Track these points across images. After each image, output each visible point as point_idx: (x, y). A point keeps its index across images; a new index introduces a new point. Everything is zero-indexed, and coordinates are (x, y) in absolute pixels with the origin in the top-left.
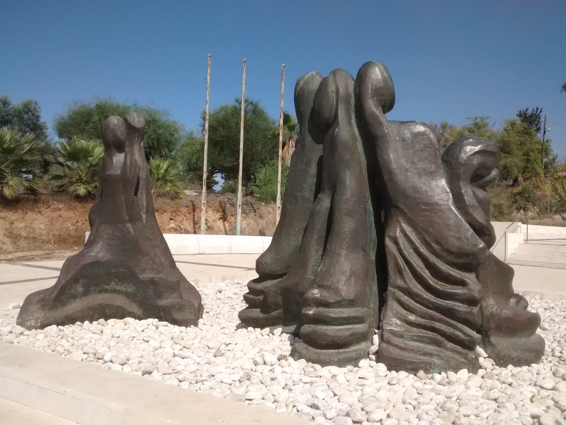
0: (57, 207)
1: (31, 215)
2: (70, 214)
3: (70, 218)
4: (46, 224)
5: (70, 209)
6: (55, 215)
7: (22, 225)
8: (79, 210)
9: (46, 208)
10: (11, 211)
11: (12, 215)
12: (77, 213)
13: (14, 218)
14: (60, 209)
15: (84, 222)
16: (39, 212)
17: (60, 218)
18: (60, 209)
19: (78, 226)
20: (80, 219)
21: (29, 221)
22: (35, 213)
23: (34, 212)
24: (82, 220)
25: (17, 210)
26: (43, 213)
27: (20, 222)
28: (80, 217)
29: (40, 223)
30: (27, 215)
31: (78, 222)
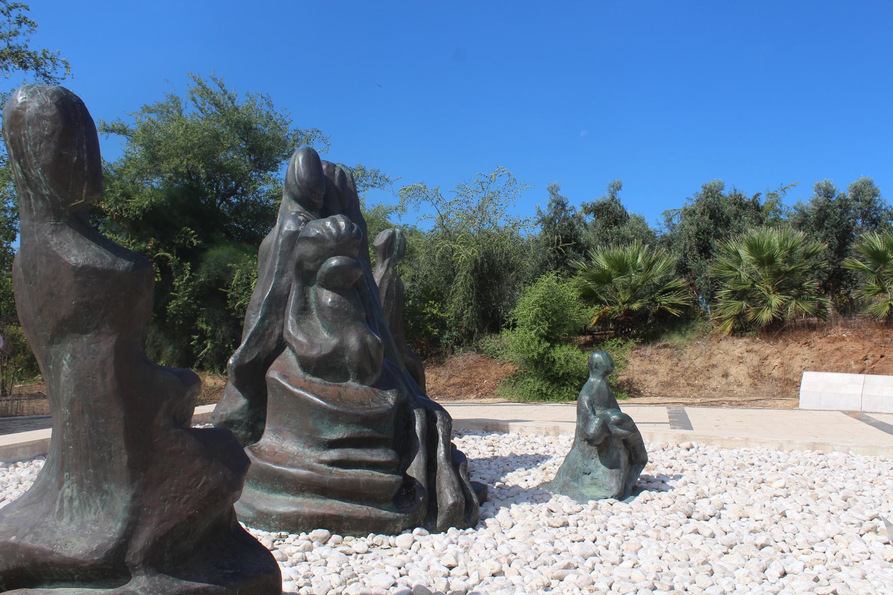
0: (839, 336)
1: (794, 347)
2: (857, 346)
3: (854, 352)
4: (811, 360)
5: (859, 338)
6: (830, 348)
7: (776, 362)
8: (875, 340)
9: (820, 338)
10: (768, 342)
11: (766, 348)
12: (868, 344)
13: (768, 352)
14: (843, 339)
15: (877, 359)
16: (806, 343)
17: (838, 353)
18: (843, 339)
19: (865, 364)
20: (871, 353)
21: (788, 357)
22: (800, 345)
23: (799, 343)
24: (873, 356)
25: (776, 339)
26: (812, 345)
27: (775, 357)
28: (871, 350)
29: (803, 359)
30: (787, 348)
31: (867, 359)
